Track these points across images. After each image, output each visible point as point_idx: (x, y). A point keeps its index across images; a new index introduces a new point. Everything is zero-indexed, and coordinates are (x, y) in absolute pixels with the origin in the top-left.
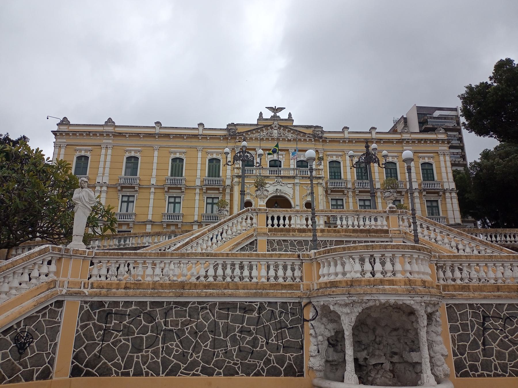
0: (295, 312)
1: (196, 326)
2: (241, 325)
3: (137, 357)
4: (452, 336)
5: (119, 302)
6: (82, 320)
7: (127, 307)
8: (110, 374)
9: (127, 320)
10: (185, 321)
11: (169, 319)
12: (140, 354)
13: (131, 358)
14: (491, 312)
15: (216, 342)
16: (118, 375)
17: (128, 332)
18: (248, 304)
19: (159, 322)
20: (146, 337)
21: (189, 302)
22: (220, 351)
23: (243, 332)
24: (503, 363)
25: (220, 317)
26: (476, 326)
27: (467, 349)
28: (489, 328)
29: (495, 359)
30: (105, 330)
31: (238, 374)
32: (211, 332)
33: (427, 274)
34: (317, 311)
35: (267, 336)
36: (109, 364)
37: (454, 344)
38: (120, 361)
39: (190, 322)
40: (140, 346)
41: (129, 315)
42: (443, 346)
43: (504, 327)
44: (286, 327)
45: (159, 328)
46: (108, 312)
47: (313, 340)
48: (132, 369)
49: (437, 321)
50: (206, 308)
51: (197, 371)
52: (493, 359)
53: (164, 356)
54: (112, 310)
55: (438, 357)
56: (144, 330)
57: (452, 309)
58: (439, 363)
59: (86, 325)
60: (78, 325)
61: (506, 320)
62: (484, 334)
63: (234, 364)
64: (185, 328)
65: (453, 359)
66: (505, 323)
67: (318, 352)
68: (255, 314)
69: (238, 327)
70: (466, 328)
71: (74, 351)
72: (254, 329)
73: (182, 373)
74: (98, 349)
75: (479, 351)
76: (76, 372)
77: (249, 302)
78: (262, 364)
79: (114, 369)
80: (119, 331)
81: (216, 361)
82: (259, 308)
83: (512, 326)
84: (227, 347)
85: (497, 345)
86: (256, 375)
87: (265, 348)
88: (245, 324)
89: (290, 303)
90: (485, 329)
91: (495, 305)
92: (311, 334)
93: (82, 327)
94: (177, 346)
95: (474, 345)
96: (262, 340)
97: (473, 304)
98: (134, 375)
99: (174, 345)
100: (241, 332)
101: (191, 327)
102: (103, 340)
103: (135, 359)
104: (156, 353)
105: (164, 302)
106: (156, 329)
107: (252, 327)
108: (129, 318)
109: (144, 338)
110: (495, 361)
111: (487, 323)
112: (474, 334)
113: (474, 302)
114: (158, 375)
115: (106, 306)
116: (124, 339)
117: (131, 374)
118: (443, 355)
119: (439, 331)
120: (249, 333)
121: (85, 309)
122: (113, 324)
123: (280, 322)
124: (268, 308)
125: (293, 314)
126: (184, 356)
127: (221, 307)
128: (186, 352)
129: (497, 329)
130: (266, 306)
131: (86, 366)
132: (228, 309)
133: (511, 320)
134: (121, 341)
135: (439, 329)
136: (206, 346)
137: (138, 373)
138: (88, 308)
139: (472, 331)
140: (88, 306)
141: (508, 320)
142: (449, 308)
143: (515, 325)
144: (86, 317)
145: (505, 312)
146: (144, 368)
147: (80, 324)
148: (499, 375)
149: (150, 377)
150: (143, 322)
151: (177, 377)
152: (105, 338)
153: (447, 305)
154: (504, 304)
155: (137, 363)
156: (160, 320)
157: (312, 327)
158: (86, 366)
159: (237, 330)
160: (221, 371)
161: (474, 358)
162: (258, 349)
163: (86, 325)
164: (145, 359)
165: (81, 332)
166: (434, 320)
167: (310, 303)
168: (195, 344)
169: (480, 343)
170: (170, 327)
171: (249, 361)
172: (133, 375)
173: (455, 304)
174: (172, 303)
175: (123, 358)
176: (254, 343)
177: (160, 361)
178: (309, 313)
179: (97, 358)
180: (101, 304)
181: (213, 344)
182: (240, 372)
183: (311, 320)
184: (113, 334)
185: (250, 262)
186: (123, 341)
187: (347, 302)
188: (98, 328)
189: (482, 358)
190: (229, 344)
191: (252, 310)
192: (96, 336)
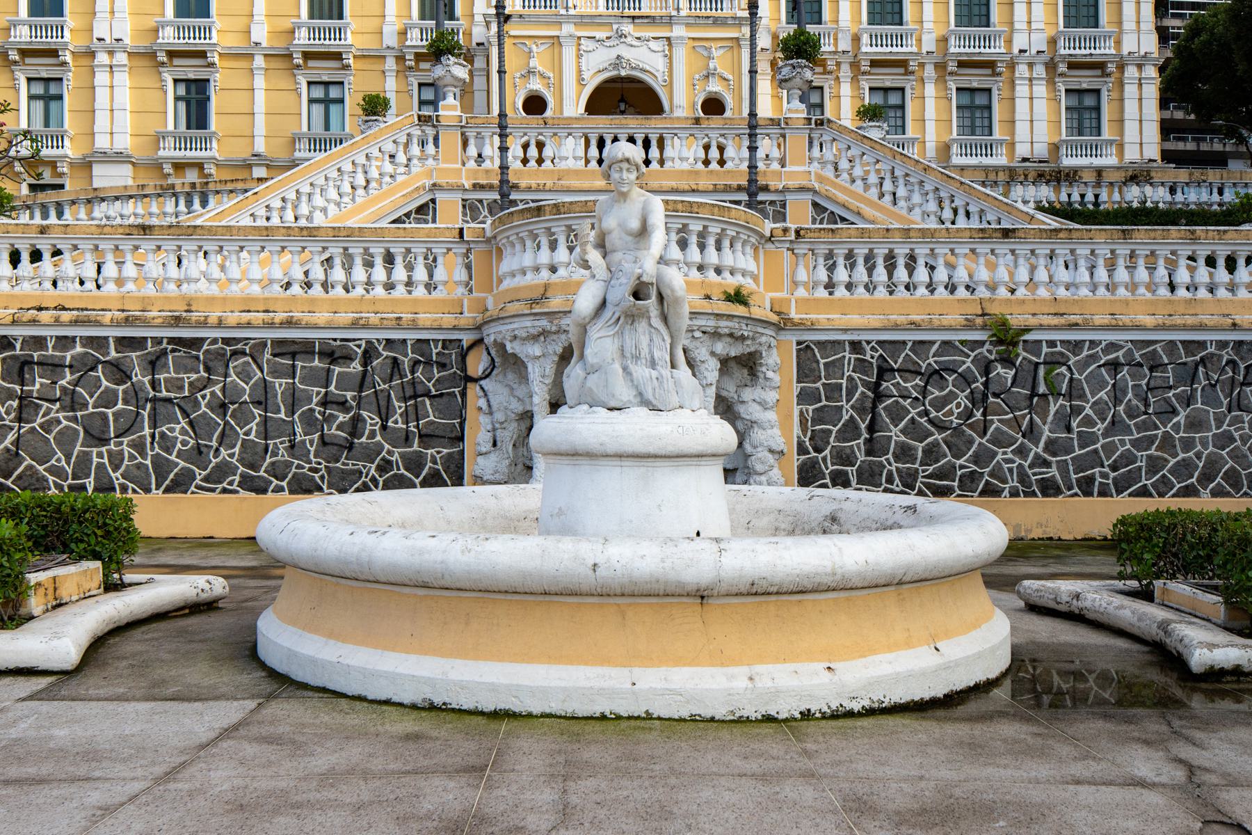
0: (448, 362)
1: (224, 390)
2: (323, 390)
4: (801, 413)
5: (45, 338)
9: (69, 377)
10: (198, 380)
11: (161, 377)
12: (104, 449)
13: (85, 459)
14: (900, 361)
15: (269, 424)
17: (72, 402)
18: (338, 343)
19: (139, 381)
20: (114, 414)
21: (203, 340)
22: (280, 444)
23: (329, 406)
24: (908, 468)
25: (276, 373)
26: (861, 389)
27: (832, 440)
28: (889, 393)
29: (892, 460)
30: (21, 398)
31: (320, 489)
32: (258, 403)
33: (744, 273)
34: (493, 360)
35: (385, 413)
36: (41, 468)
37: (804, 431)
38: (63, 463)
39: (209, 382)
40: (103, 432)
41: (71, 366)
42: (776, 431)
43: (924, 392)
44: (427, 394)
45: (141, 395)
46: (22, 359)
47: (484, 420)
48: (92, 479)
49: (766, 379)
50: (244, 353)
51: (231, 483)
52: (887, 460)
53: (158, 454)
54: (32, 356)
55: (759, 455)
56: (108, 400)
57: (809, 353)
58: (759, 468)
61: (931, 376)
62: (874, 407)
63: (311, 469)
64: (198, 395)
65: (795, 461)
66: (927, 383)
67: (495, 444)
68: (356, 367)
69: (318, 393)
70: (836, 395)
72: (354, 398)
73: (197, 487)
75: (858, 445)
77: (342, 340)
78: (373, 471)
79: (51, 478)
80: (53, 401)
81: (273, 464)
82: (366, 352)
83: (942, 389)
84: (295, 434)
85: (901, 431)
86: (357, 490)
87: (379, 438)
88: (332, 388)
89: (436, 341)
90: (879, 396)
91: (910, 344)
92: (480, 409)
94: (183, 432)
95: (850, 430)
96: (371, 420)
97: (860, 342)
99: (178, 429)
100: (324, 403)
101: (213, 393)
103: (95, 460)
104: (139, 446)
105: (145, 338)
106: (135, 395)
107: (349, 395)
108: (72, 374)
109: (111, 418)
110: (890, 464)
111: (885, 384)
112: (852, 407)
113: (863, 337)
114: (147, 490)
115: (18, 346)
116: (65, 418)
118: (771, 451)
119: (768, 400)
120: (343, 405)
122: (37, 386)
123: (413, 383)
124: (385, 354)
125: (442, 366)
126: (200, 453)
127: (277, 351)
128: (206, 446)
129: (904, 397)
130: (380, 349)
132: (293, 356)
133: (942, 377)
134: (59, 422)
135: (771, 396)
136: (247, 434)
139: (848, 401)
141: (936, 377)
142: (804, 350)
143: (950, 387)
145: (931, 360)
148: (892, 491)
151: (188, 495)
152: (24, 416)
153: (799, 343)
154: (933, 343)
155: (100, 467)
156: (140, 377)
157: (481, 394)
159: (315, 400)
160: (284, 484)
161: (845, 458)
162: (364, 439)
166: (762, 376)
167: (480, 341)
168: (224, 429)
169: (863, 426)
170: (164, 394)
171: (344, 464)
173: (820, 344)
174: (165, 341)
175: (68, 457)
176: (355, 426)
177: (148, 462)
178: (477, 364)
181: (262, 429)
182: (325, 487)
183: (481, 379)
184: (38, 407)
185: (346, 249)
186: (65, 423)
187: (534, 331)
189: (861, 457)
190: (299, 430)
191: (348, 358)
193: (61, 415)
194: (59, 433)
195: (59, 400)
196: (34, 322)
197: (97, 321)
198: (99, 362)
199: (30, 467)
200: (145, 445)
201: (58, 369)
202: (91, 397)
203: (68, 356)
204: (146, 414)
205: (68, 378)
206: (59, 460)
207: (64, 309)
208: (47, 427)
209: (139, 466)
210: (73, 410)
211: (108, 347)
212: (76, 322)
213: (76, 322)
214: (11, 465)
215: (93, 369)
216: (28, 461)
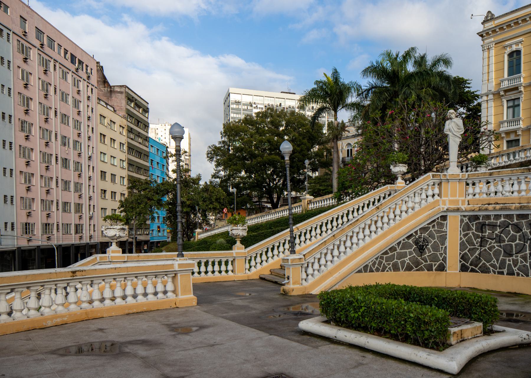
3: (509, 261)
5: (490, 215)
6: (464, 231)
7: (497, 219)
8: (489, 272)
9: (498, 230)
12: (511, 258)
16: (495, 272)
17: (500, 240)
19: (525, 232)
20: (515, 245)
30: (481, 238)
36: (488, 264)
40: (511, 252)
41: (499, 226)
45: (526, 237)
48: (506, 270)
56: (513, 239)
59: (467, 234)
60: (461, 234)
71: (460, 253)
74: (478, 252)
76: (464, 268)
79: (491, 268)
80: (492, 239)
93: (465, 236)
98: (508, 274)
102: (481, 246)
103: (508, 262)
104: (525, 258)
106: (524, 238)
108: (500, 229)
109: (514, 246)
115: (481, 219)
116: (497, 246)
117: (505, 274)
121: (465, 222)
122: (487, 233)
131: (471, 265)
134: (495, 247)
137: (511, 273)
138: (467, 220)
140: (466, 219)
144: (466, 228)
146: (515, 269)
147: (462, 233)
149: (520, 277)
150: (512, 232)
152: (482, 244)
155: (509, 265)
158: (471, 265)
163: (467, 234)
164: (515, 263)
165: (464, 239)
172: (508, 274)
175: (497, 261)
177: (528, 264)
179: (478, 259)
180: (477, 217)
184: (488, 241)
186: (497, 247)
188: (476, 237)
192: (475, 242)
193: (495, 245)
194: (495, 251)
195: (495, 239)
196: (486, 210)
197: (509, 208)
198: (510, 224)
199: (484, 264)
200: (527, 257)
201: (495, 227)
202: (507, 238)
203: (499, 222)
204: (528, 245)
205: (498, 231)
206: (494, 262)
207: (498, 204)
208: (490, 249)
209: (524, 266)
210: (500, 243)
211: (513, 218)
212: (501, 209)
213: (501, 209)
214: (478, 262)
215: (508, 227)
216: (484, 261)
